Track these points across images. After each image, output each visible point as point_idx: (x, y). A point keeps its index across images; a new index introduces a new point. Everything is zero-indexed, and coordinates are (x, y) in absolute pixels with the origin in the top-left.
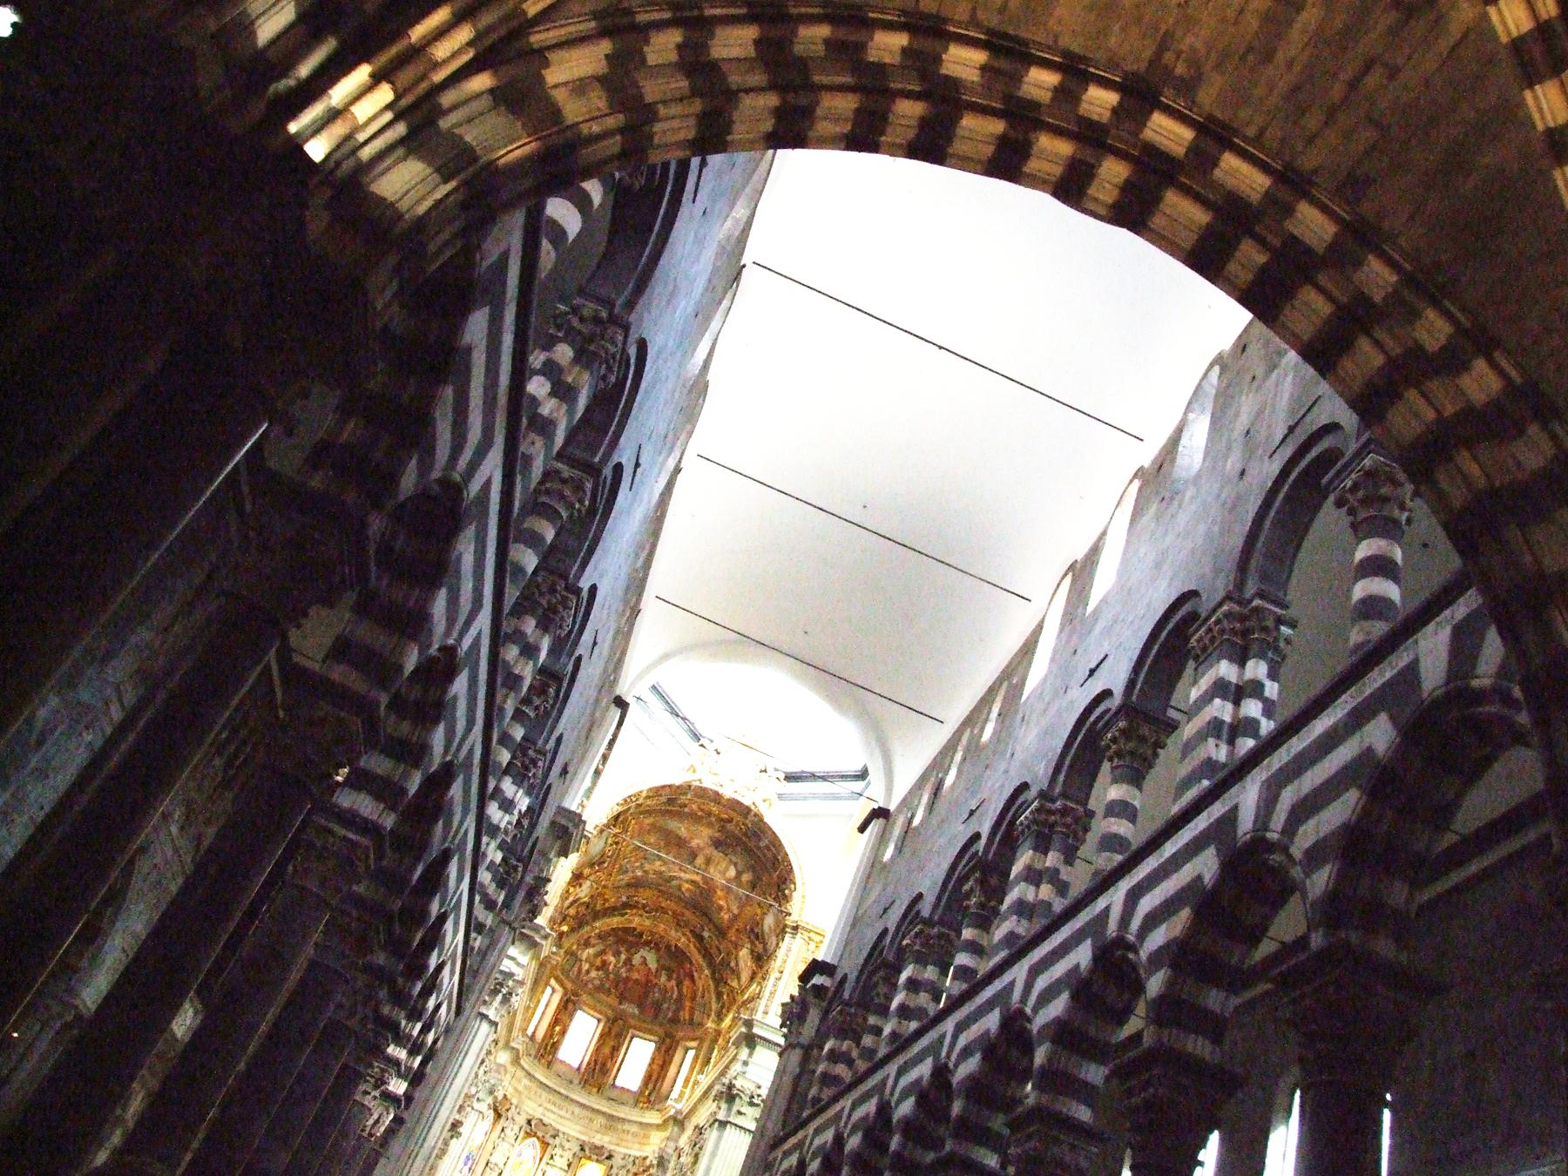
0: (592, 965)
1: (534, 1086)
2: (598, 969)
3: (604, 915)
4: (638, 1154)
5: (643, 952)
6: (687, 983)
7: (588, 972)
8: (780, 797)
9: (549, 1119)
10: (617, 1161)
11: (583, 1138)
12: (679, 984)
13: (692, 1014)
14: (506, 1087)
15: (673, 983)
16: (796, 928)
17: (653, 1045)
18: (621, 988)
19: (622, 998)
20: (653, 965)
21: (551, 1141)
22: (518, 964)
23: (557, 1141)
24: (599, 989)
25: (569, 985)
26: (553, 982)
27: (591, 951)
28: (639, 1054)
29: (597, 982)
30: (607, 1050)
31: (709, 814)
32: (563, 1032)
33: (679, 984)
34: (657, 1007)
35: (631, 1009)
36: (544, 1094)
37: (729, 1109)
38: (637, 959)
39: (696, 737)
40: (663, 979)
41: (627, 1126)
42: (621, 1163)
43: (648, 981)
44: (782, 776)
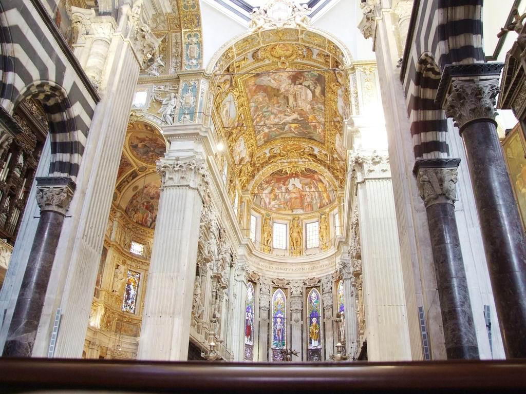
0: (270, 199)
1: (266, 264)
2: (274, 200)
3: (263, 167)
4: (332, 272)
5: (292, 181)
6: (320, 185)
7: (270, 203)
8: (311, 16)
9: (281, 276)
10: (324, 281)
11: (304, 278)
12: (316, 187)
13: (328, 197)
14: (252, 268)
15: (313, 189)
16: (353, 69)
17: (317, 223)
18: (290, 205)
19: (292, 209)
20: (299, 186)
21: (287, 287)
22: (197, 153)
23: (291, 285)
24: (279, 209)
25: (263, 212)
26: (253, 212)
27: (266, 191)
28: (312, 231)
29: (276, 206)
30: (295, 235)
31: (280, 58)
32: (270, 234)
33: (316, 187)
34: (310, 205)
35: (300, 211)
36: (274, 267)
37: (363, 174)
38: (291, 187)
39: (249, 9)
40: (308, 190)
41: (321, 263)
42: (327, 280)
43: (301, 196)
44: (306, 6)
